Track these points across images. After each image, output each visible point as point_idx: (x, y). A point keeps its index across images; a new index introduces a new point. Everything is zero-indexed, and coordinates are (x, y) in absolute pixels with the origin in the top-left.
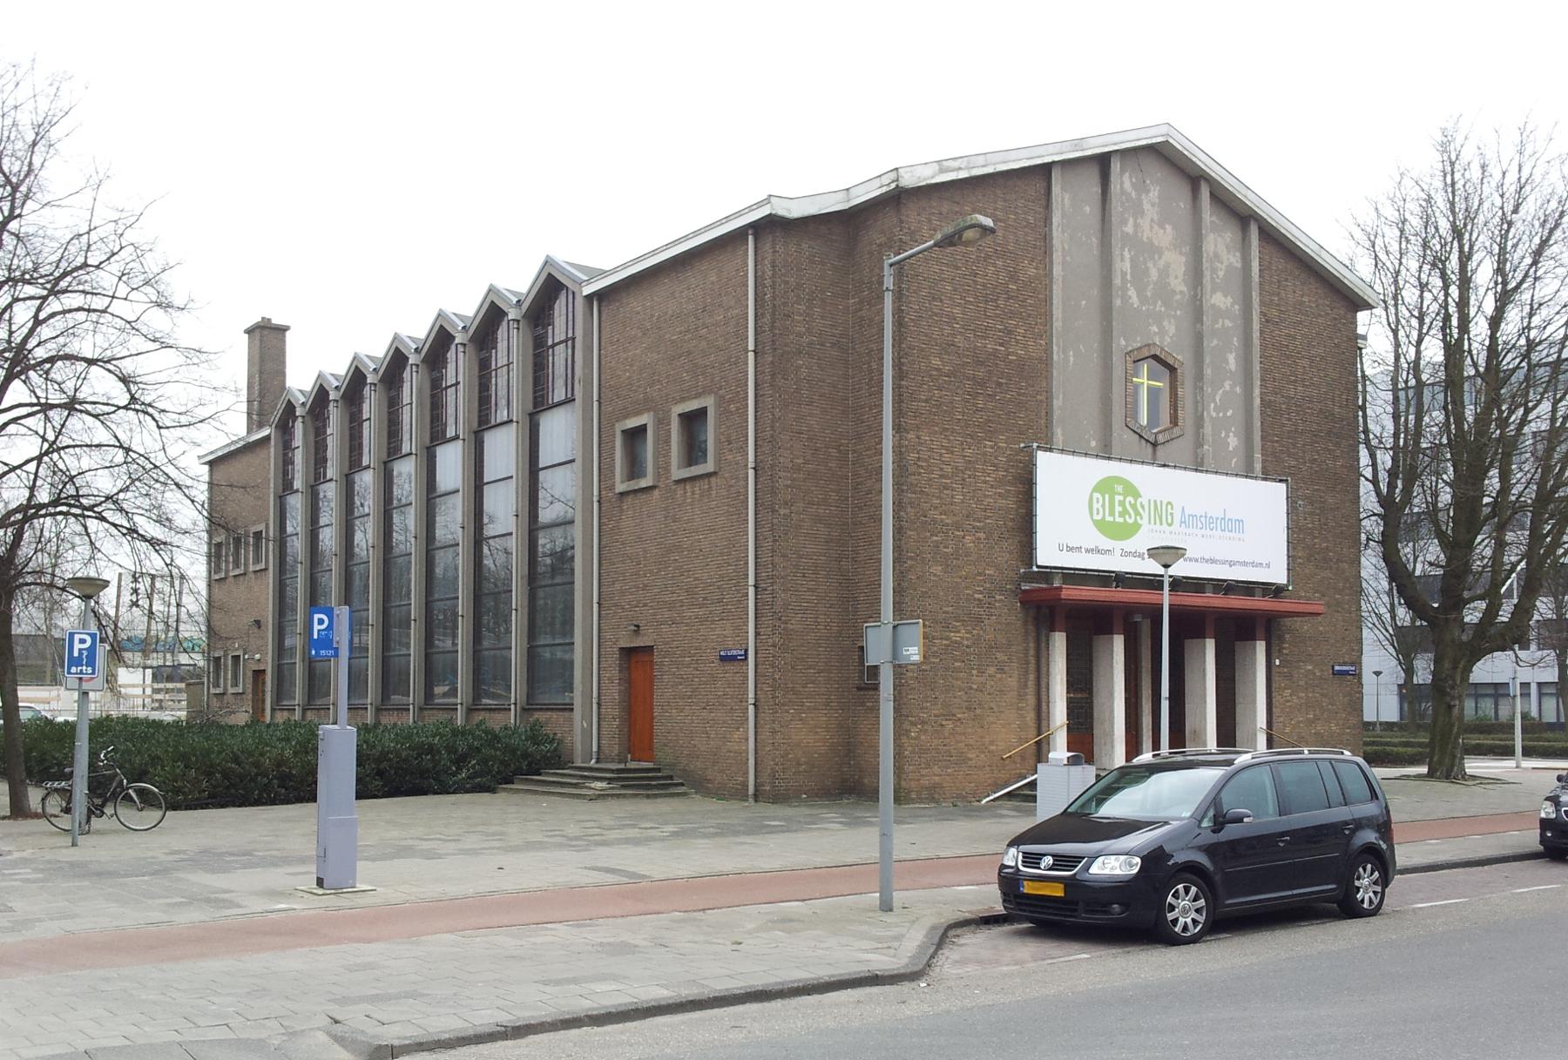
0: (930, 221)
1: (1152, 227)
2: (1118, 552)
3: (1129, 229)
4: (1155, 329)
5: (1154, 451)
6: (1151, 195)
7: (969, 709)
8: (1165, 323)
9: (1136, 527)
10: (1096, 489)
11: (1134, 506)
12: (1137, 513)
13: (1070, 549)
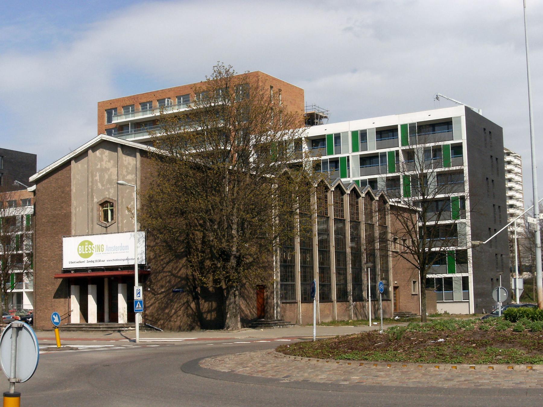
0: (42, 186)
1: (106, 163)
2: (86, 262)
3: (99, 166)
4: (107, 193)
5: (106, 230)
6: (106, 154)
7: (52, 307)
8: (110, 190)
9: (92, 254)
10: (79, 245)
11: (91, 248)
12: (92, 249)
13: (72, 263)
